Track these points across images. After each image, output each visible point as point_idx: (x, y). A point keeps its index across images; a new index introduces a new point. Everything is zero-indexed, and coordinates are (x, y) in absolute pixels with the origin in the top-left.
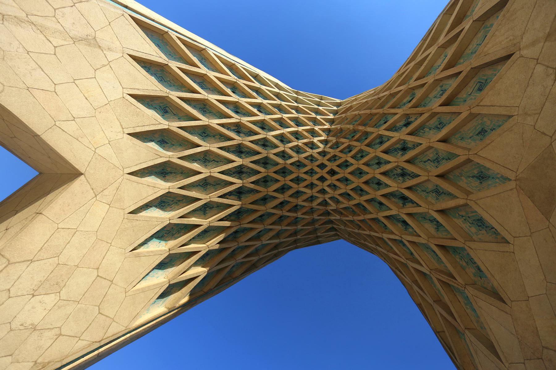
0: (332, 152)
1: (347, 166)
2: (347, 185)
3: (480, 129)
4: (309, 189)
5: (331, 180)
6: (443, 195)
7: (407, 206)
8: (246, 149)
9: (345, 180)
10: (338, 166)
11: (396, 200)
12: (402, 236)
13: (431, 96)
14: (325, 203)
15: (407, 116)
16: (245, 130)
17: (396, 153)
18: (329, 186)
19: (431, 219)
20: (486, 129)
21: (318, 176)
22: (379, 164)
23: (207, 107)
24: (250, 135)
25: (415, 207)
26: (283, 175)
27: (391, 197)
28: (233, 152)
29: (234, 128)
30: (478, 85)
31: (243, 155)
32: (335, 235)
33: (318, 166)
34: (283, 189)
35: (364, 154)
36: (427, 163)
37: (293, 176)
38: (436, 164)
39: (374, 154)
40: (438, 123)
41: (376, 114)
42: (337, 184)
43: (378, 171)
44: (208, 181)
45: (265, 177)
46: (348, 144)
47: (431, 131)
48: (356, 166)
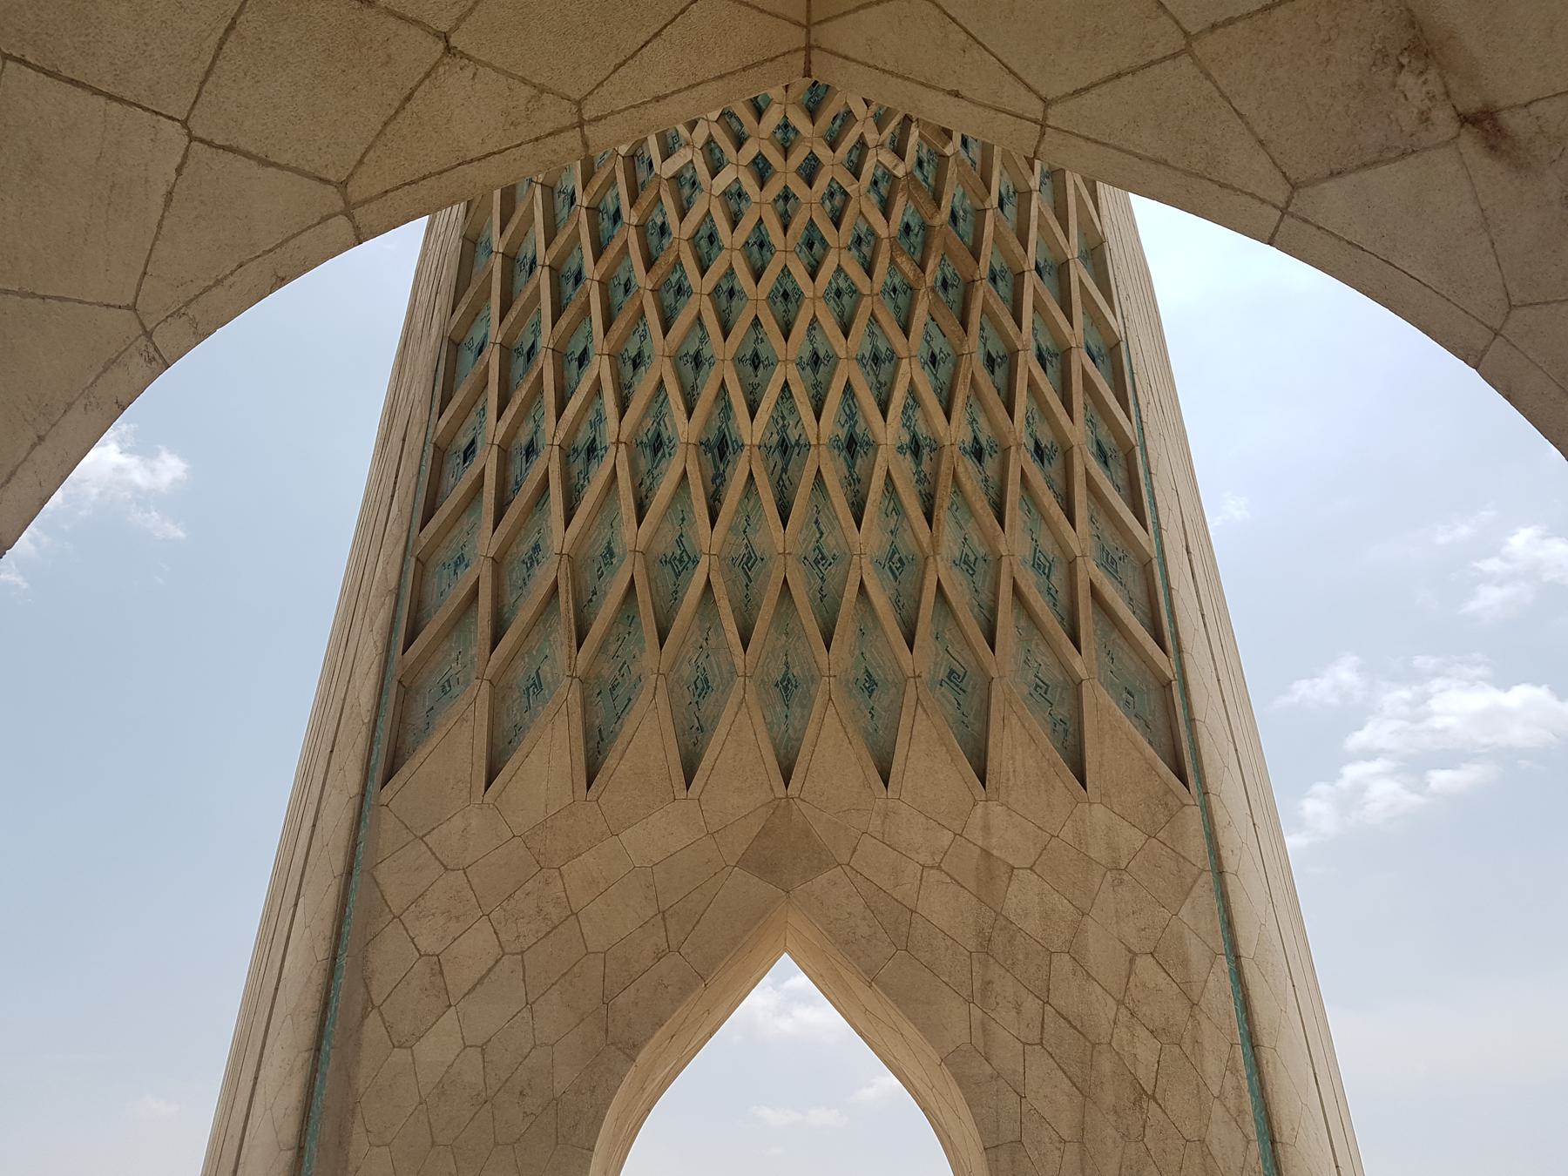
1: (810, 246)
3: (876, 677)
5: (761, 202)
6: (745, 581)
7: (703, 458)
12: (622, 447)
13: (970, 527)
15: (937, 448)
25: (705, 488)
30: (960, 671)
35: (846, 299)
38: (811, 559)
39: (842, 354)
40: (903, 553)
41: (964, 324)
43: (793, 374)
48: (808, 294)
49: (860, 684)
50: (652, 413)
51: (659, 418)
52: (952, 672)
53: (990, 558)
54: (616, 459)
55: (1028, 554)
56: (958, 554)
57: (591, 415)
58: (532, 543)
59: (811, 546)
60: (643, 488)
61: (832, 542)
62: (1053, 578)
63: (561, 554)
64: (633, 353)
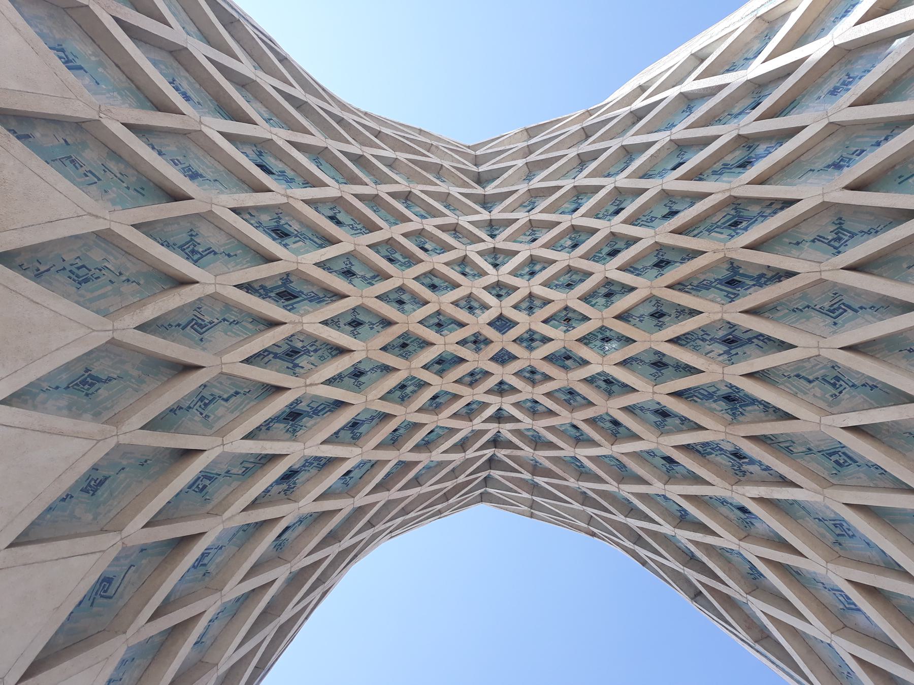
0: (479, 393)
1: (440, 361)
2: (438, 313)
3: (99, 492)
4: (539, 297)
5: (479, 323)
6: (183, 322)
8: (714, 405)
9: (440, 323)
10: (462, 360)
11: (306, 289)
14: (496, 257)
16: (719, 459)
17: (314, 405)
18: (485, 307)
19: (211, 255)
20: (85, 495)
21: (514, 333)
22: (357, 373)
23: (831, 538)
24: (705, 444)
26: (608, 334)
27: (321, 295)
28: (754, 401)
29: (751, 468)
31: (724, 390)
32: (487, 158)
33: (516, 358)
34: (610, 290)
35: (398, 393)
36: (232, 392)
37: (582, 329)
38: (206, 393)
40: (210, 489)
42: (462, 315)
44: (829, 321)
45: (660, 327)
46: (441, 416)
47: (224, 468)
50: (304, 230)
51: (300, 237)
53: (207, 579)
54: (278, 193)
57: (290, 173)
58: (190, 93)
59: (217, 392)
60: (248, 216)
61: (220, 411)
63: (201, 122)
64: (340, 217)
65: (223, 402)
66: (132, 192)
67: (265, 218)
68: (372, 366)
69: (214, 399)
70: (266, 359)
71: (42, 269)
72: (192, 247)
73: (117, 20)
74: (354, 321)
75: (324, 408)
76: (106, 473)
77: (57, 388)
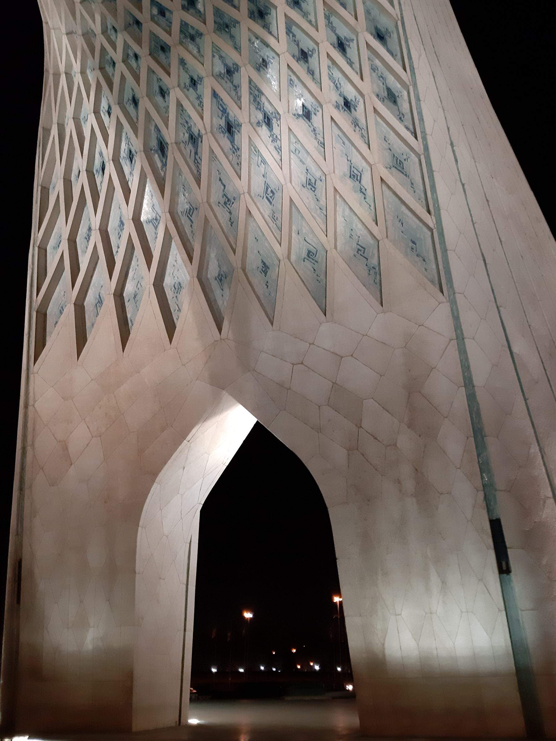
17: (220, 113)
30: (314, 251)
36: (220, 183)
38: (222, 202)
40: (272, 187)
49: (261, 267)
52: (309, 252)
55: (346, 169)
56: (304, 180)
58: (87, 227)
59: (221, 196)
62: (363, 182)
63: (95, 230)
65: (226, 188)
66: (138, 263)
67: (127, 169)
68: (185, 73)
69: (225, 195)
70: (199, 160)
71: (177, 308)
72: (155, 221)
73: (73, 286)
74: (161, 93)
75: (221, 105)
76: (261, 262)
77: (222, 296)
